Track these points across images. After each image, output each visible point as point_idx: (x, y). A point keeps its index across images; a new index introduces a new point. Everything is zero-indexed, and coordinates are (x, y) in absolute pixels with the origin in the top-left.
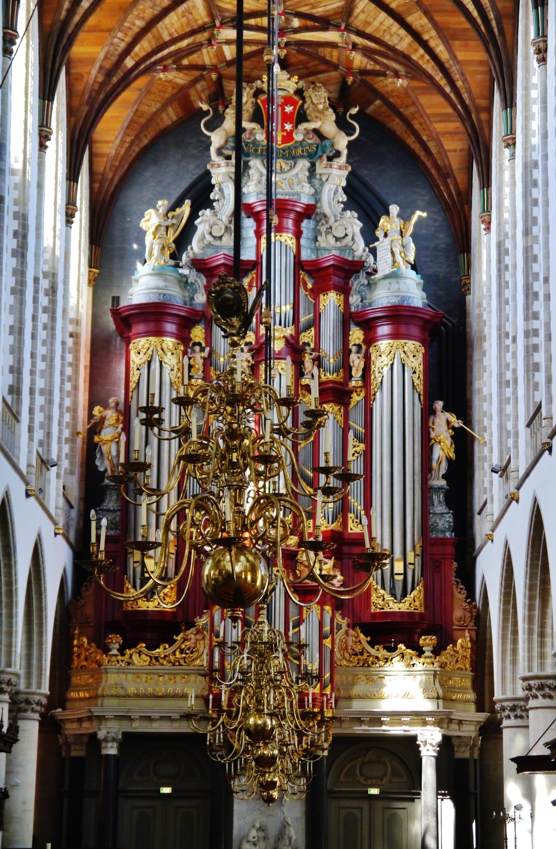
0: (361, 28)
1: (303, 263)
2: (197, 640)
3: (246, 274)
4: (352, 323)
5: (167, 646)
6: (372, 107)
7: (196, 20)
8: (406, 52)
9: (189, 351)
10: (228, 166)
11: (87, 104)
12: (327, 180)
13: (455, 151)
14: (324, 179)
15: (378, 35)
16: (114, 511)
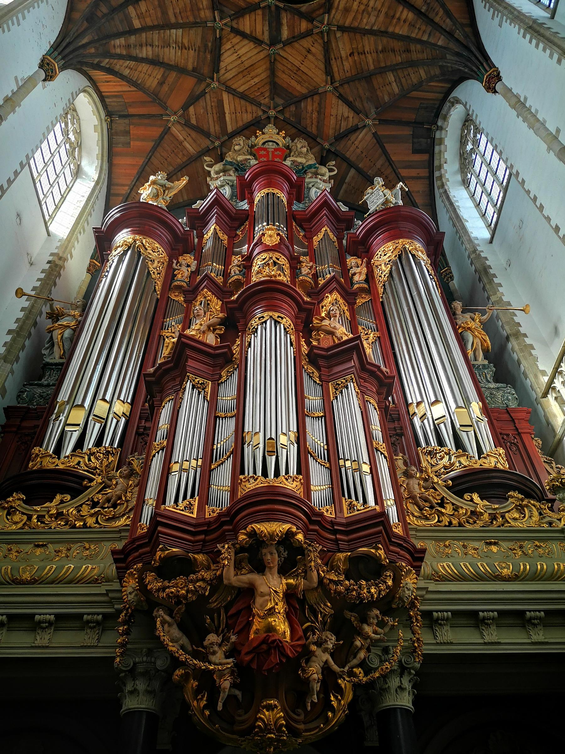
0: (341, 23)
1: (294, 213)
2: (128, 486)
3: (239, 227)
4: (348, 256)
5: (69, 497)
6: (344, 186)
7: (199, 10)
8: (383, 29)
9: (175, 262)
10: (224, 175)
11: (87, 20)
12: (313, 186)
13: (419, 192)
14: (310, 185)
15: (356, 24)
16: (48, 385)
